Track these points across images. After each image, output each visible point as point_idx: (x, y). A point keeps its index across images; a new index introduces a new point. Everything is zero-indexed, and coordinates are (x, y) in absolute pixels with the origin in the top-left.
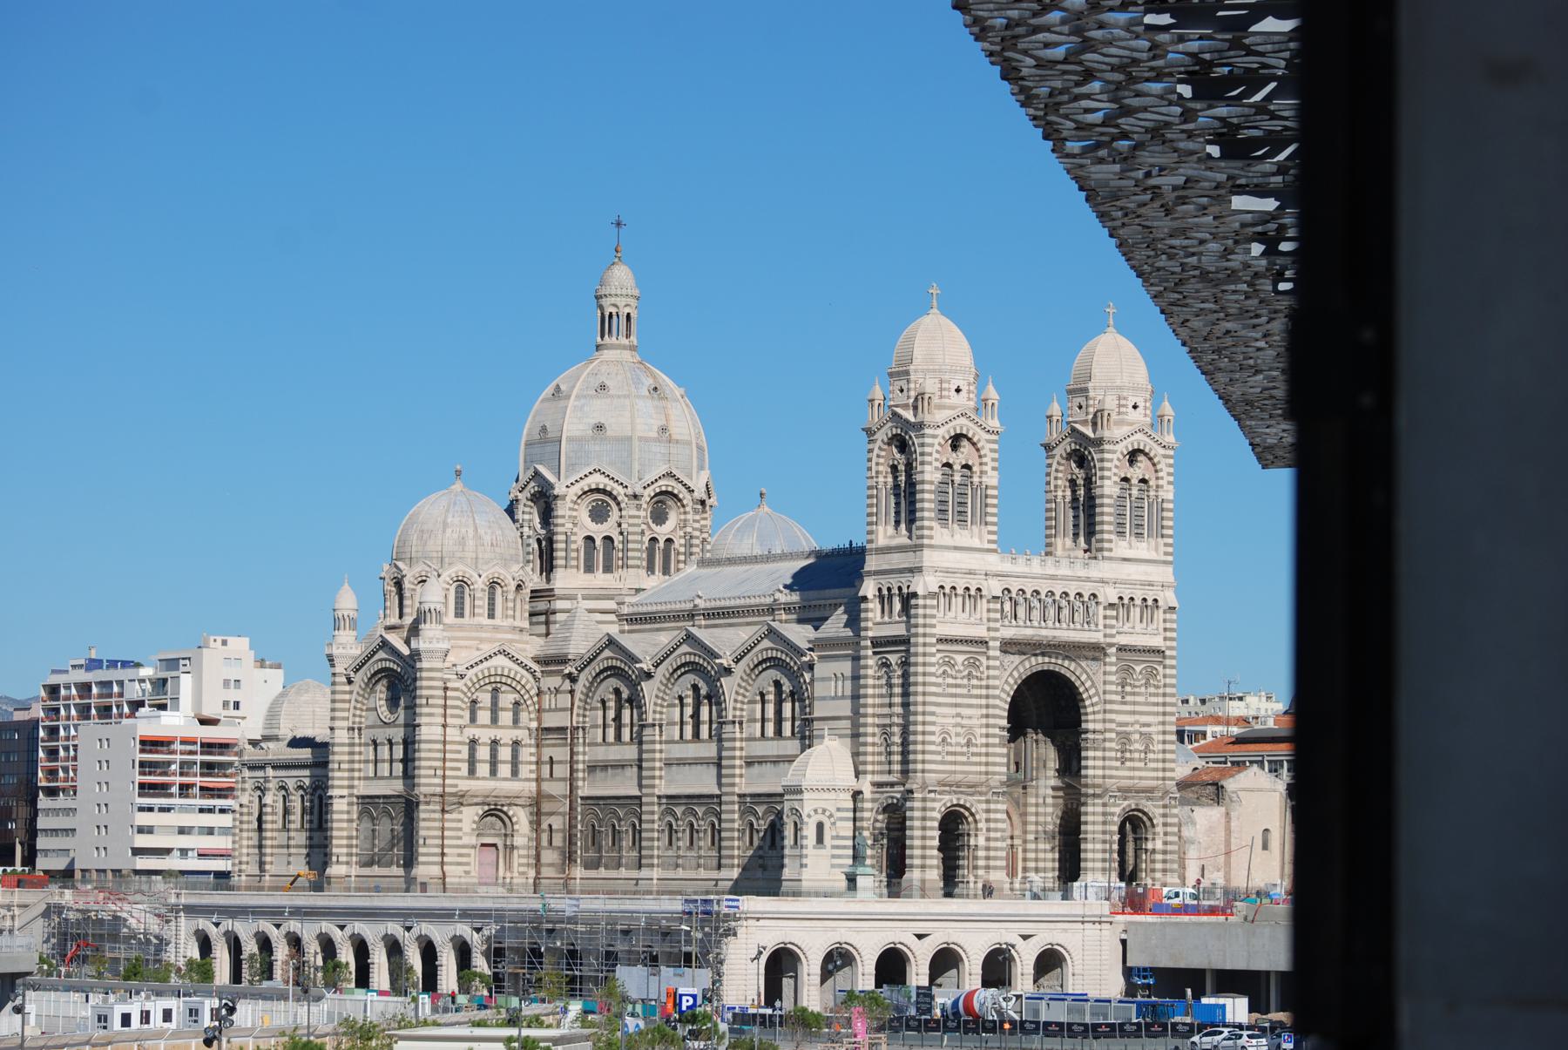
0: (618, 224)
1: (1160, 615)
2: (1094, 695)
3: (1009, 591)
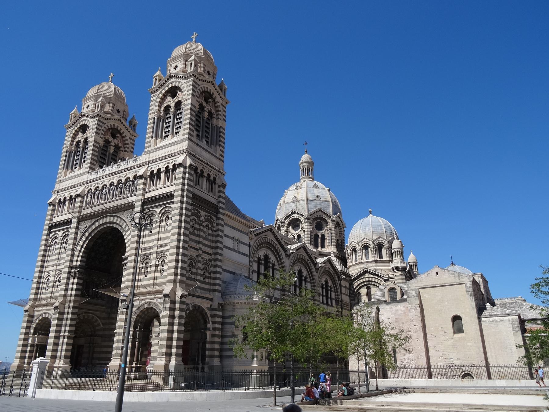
0: (306, 144)
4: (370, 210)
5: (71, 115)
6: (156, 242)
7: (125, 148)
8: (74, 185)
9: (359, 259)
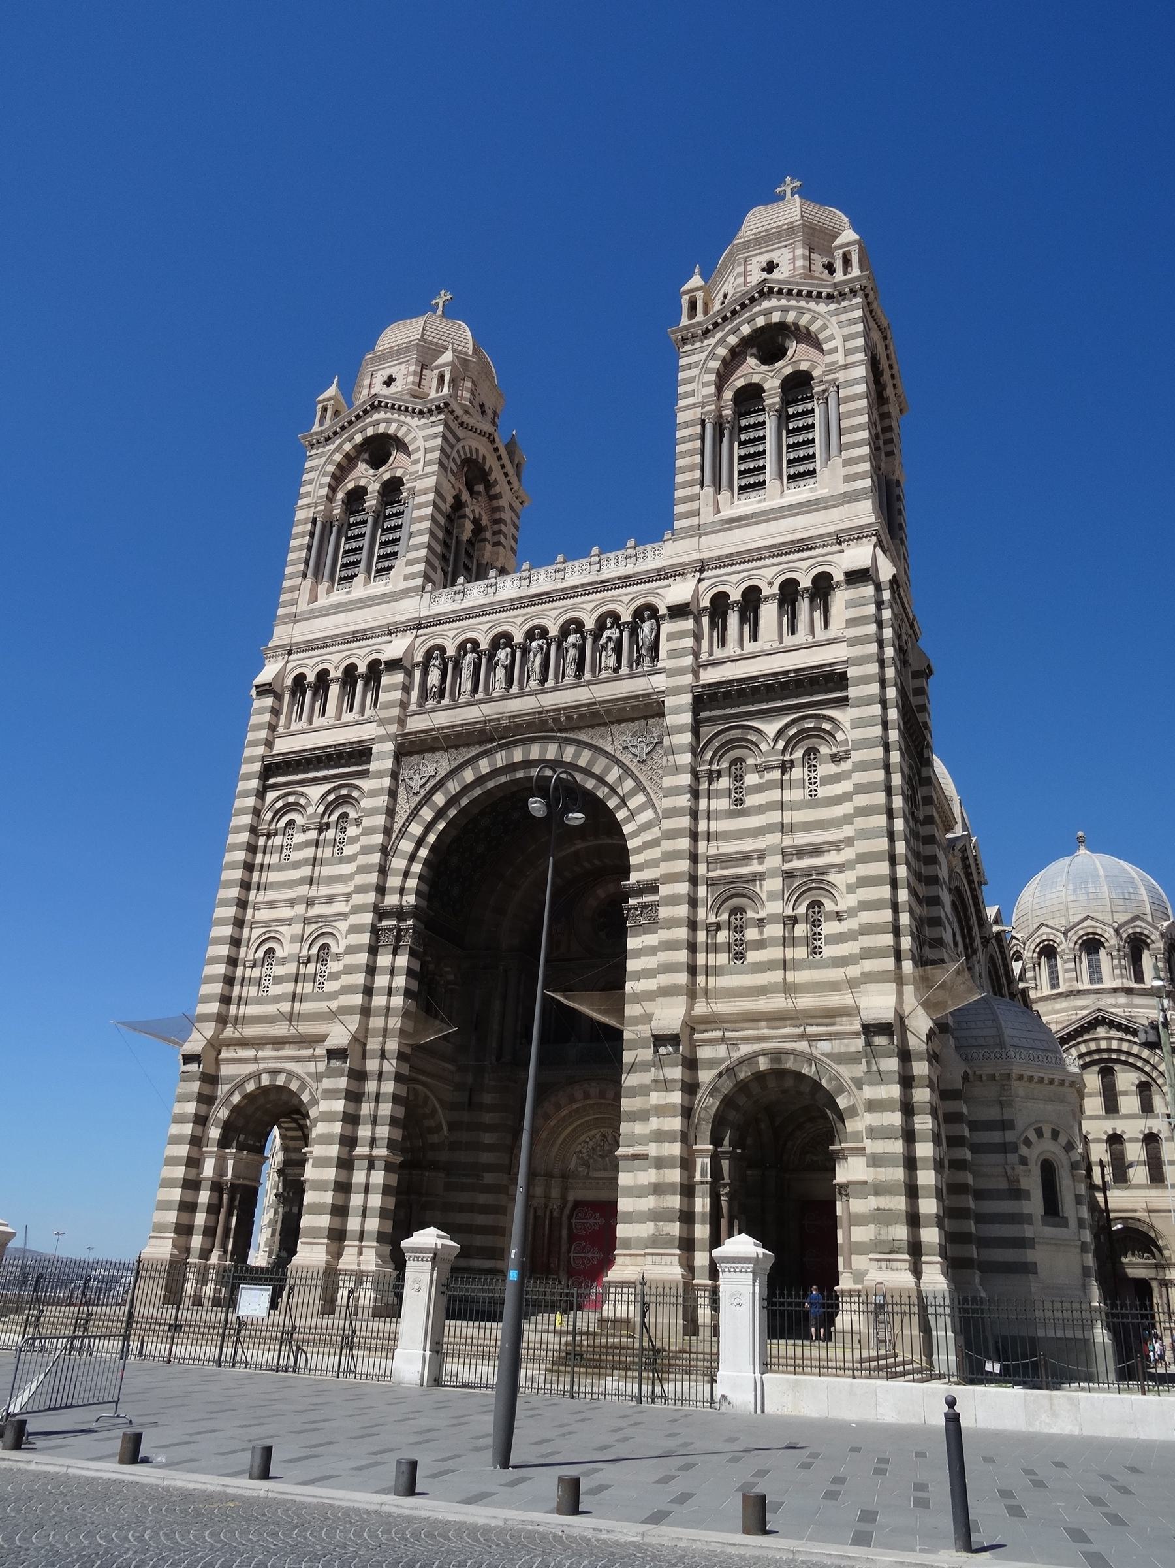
1: (840, 598)
2: (641, 808)
3: (443, 650)
4: (1080, 833)
5: (320, 402)
6: (773, 838)
7: (495, 533)
8: (365, 630)
9: (1071, 980)
